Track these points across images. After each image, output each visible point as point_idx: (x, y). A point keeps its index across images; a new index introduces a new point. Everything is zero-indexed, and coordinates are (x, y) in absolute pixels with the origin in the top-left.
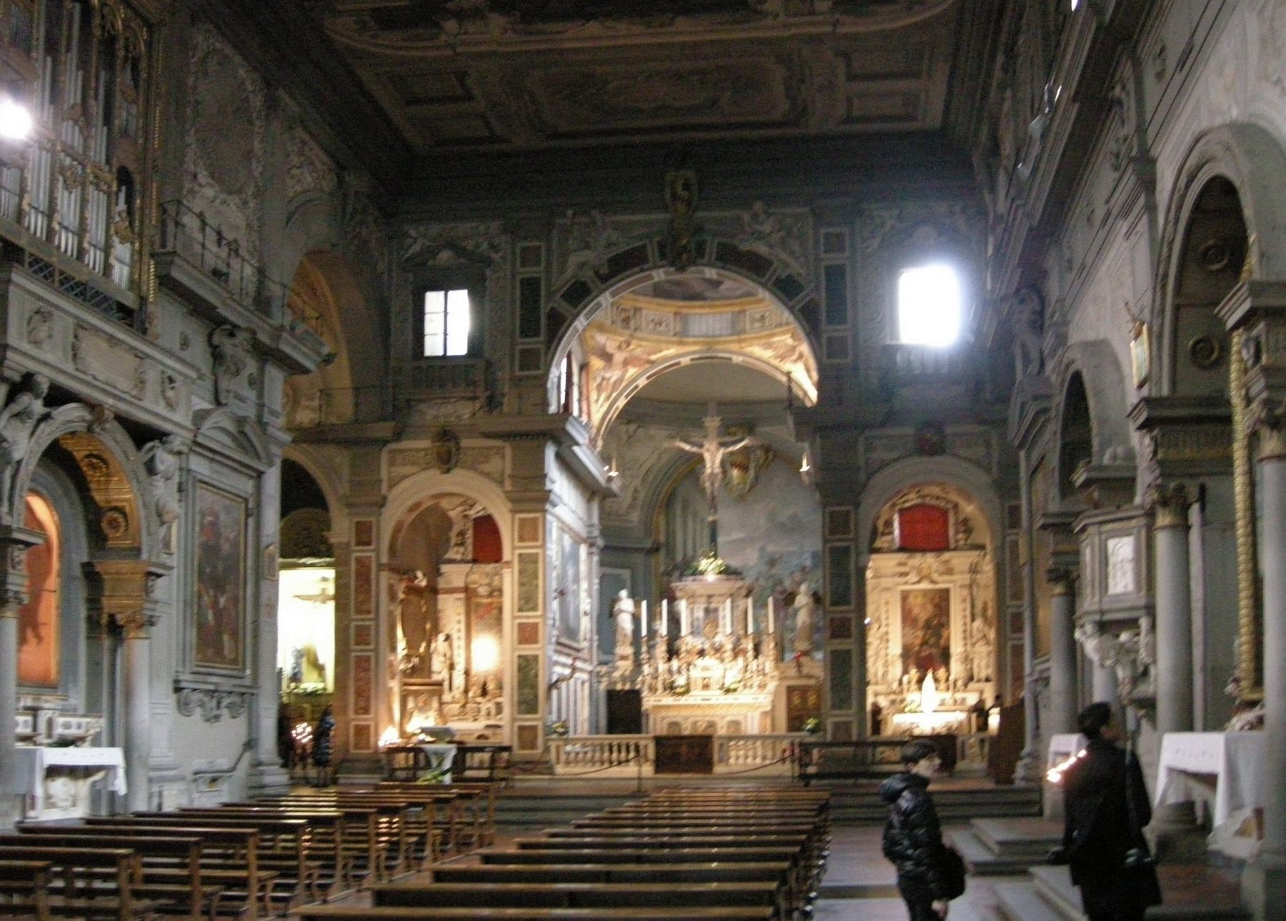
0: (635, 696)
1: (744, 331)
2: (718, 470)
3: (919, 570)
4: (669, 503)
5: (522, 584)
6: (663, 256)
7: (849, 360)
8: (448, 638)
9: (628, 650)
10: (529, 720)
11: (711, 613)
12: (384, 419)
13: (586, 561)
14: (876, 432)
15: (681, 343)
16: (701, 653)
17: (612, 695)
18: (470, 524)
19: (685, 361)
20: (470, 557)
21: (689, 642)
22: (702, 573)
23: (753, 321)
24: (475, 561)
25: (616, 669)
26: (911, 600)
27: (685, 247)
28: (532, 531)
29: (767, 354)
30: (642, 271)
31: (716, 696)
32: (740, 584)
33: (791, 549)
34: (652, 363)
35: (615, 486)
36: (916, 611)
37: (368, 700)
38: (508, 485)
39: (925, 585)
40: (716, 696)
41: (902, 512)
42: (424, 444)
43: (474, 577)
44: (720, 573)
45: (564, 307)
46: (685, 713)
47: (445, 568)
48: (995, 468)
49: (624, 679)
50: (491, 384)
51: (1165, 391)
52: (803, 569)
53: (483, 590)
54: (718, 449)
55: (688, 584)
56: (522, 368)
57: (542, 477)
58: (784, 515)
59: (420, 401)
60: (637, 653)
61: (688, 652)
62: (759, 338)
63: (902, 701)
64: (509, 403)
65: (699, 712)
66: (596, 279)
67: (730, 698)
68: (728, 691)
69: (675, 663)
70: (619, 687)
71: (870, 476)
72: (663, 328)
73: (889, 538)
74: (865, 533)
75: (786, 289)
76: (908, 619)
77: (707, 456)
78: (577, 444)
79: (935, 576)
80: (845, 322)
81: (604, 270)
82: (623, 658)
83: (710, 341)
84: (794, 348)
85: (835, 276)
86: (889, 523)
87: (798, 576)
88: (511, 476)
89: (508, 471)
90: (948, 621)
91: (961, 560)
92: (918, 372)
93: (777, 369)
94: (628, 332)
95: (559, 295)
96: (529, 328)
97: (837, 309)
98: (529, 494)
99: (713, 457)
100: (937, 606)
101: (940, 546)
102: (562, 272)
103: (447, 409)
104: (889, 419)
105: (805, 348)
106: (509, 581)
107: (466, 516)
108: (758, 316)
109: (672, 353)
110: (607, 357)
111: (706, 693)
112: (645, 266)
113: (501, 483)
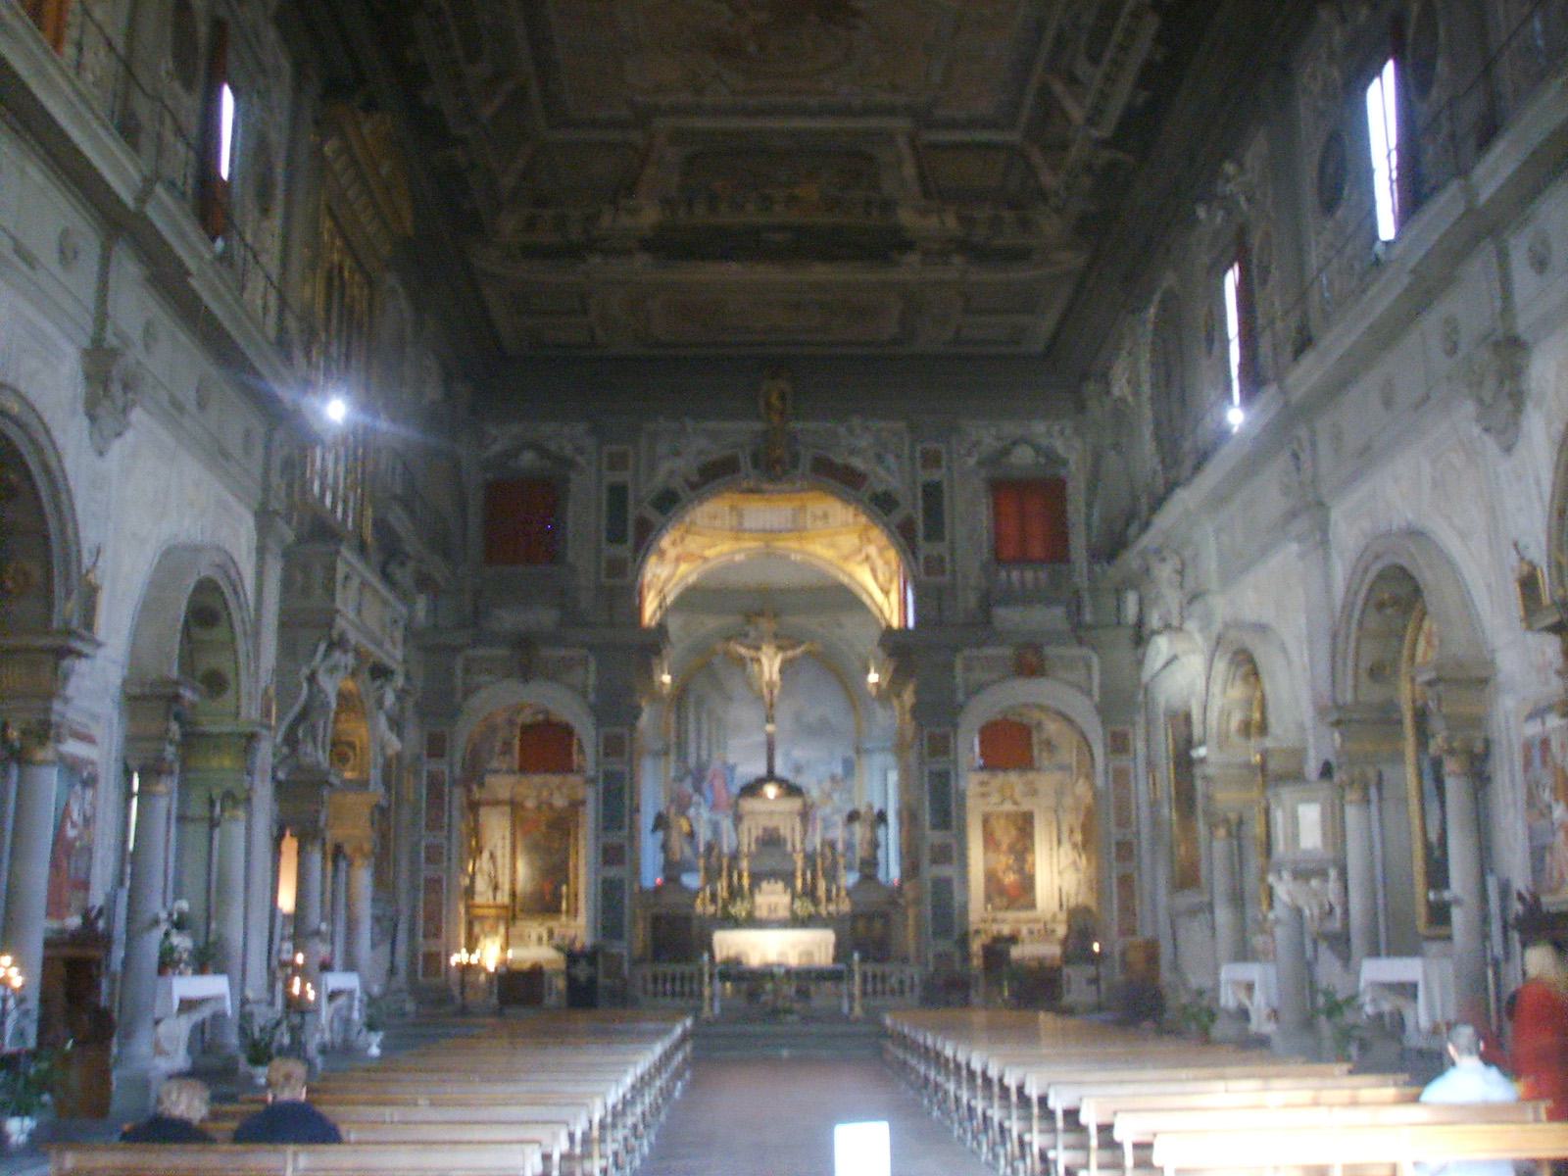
2: (776, 676)
6: (756, 465)
8: (492, 856)
15: (737, 539)
18: (518, 732)
19: (739, 558)
23: (815, 518)
26: (993, 822)
37: (439, 929)
39: (1008, 807)
45: (651, 514)
48: (1096, 691)
51: (1349, 697)
52: (833, 778)
53: (530, 804)
54: (776, 654)
66: (687, 489)
75: (881, 506)
81: (695, 478)
87: (827, 785)
90: (1033, 845)
96: (616, 535)
108: (820, 513)
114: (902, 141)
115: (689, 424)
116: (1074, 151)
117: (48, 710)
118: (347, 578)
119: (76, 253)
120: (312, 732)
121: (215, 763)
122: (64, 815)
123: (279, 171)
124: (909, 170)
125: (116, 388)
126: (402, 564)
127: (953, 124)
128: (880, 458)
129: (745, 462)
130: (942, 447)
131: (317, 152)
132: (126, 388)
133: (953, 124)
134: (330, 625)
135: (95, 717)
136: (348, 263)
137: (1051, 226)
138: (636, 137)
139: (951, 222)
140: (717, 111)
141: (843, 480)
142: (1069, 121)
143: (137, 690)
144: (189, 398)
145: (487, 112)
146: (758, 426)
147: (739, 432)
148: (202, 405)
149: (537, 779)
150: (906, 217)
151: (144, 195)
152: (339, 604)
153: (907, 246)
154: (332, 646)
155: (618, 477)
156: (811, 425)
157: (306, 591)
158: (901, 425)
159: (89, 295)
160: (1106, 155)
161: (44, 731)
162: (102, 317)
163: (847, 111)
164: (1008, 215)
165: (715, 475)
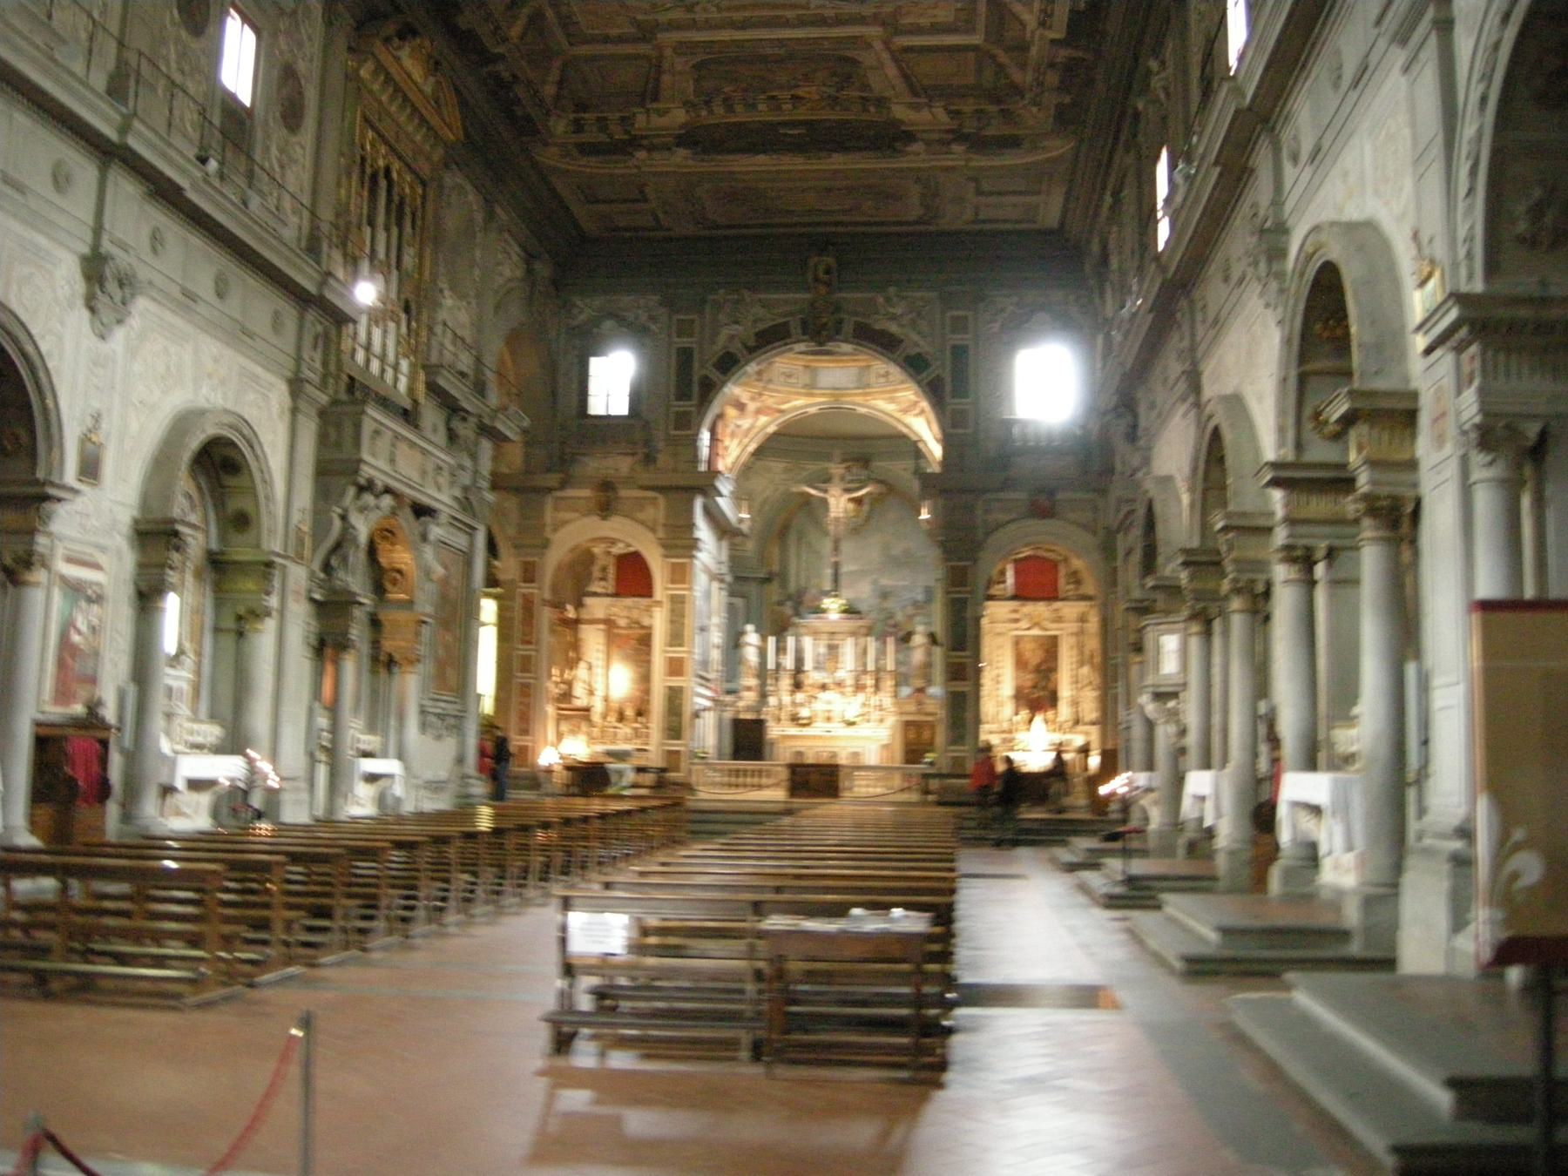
0: (758, 726)
1: (868, 386)
3: (1029, 616)
4: (783, 533)
5: (672, 622)
7: (970, 431)
9: (752, 682)
10: (675, 745)
11: (833, 649)
12: (549, 470)
13: (719, 597)
14: (994, 496)
16: (824, 687)
17: (738, 724)
19: (813, 410)
20: (611, 590)
21: (813, 676)
22: (824, 611)
24: (616, 595)
25: (740, 698)
27: (826, 324)
28: (680, 574)
29: (890, 407)
30: (786, 344)
31: (839, 730)
32: (860, 623)
33: (901, 583)
34: (782, 412)
35: (745, 527)
36: (1028, 655)
38: (661, 534)
39: (1036, 632)
40: (839, 730)
41: (1016, 561)
42: (586, 493)
43: (615, 610)
44: (845, 612)
45: (715, 375)
46: (809, 743)
47: (589, 601)
49: (748, 709)
50: (647, 443)
53: (622, 622)
55: (812, 621)
56: (677, 428)
57: (691, 526)
58: (896, 551)
59: (584, 454)
60: (763, 685)
61: (812, 686)
62: (882, 392)
63: (1011, 740)
64: (663, 459)
65: (820, 743)
66: (745, 352)
67: (850, 731)
68: (851, 724)
69: (800, 697)
70: (742, 716)
71: (988, 534)
72: (792, 380)
73: (1001, 586)
74: (982, 582)
75: (915, 366)
76: (1020, 663)
77: (832, 501)
78: (721, 495)
79: (1047, 624)
80: (967, 397)
81: (752, 343)
82: (749, 689)
83: (837, 392)
84: (916, 403)
85: (960, 353)
86: (1003, 573)
87: (910, 611)
88: (665, 525)
89: (661, 520)
91: (1071, 609)
92: (1032, 444)
93: (899, 421)
94: (761, 384)
95: (710, 362)
97: (961, 384)
98: (678, 542)
99: (839, 504)
100: (1047, 651)
101: (1051, 596)
102: (713, 342)
103: (609, 462)
104: (1006, 485)
105: (925, 404)
106: (659, 622)
107: (609, 553)
108: (882, 372)
109: (800, 404)
110: (741, 407)
111: (828, 726)
112: (788, 341)
113: (653, 530)
114: (878, 45)
115: (746, 294)
116: (1034, 51)
117: (32, 542)
118: (377, 432)
119: (68, 180)
120: (345, 560)
121: (240, 586)
122: (68, 626)
123: (311, 94)
124: (892, 71)
125: (112, 286)
126: (464, 419)
127: (917, 30)
128: (913, 323)
129: (795, 328)
130: (970, 314)
131: (351, 77)
132: (121, 285)
133: (917, 30)
134: (356, 471)
135: (103, 549)
136: (396, 165)
137: (1034, 116)
138: (643, 49)
139: (943, 117)
140: (709, 25)
141: (885, 344)
142: (1023, 25)
143: (142, 527)
144: (205, 288)
145: (515, 32)
146: (807, 296)
147: (789, 301)
148: (220, 295)
149: (629, 601)
150: (900, 112)
151: (124, 129)
152: (366, 456)
153: (910, 137)
154: (362, 489)
155: (685, 342)
156: (849, 295)
157: (338, 445)
158: (933, 295)
159: (87, 215)
160: (1064, 54)
161: (27, 561)
162: (98, 230)
163: (821, 21)
164: (992, 109)
165: (770, 339)
